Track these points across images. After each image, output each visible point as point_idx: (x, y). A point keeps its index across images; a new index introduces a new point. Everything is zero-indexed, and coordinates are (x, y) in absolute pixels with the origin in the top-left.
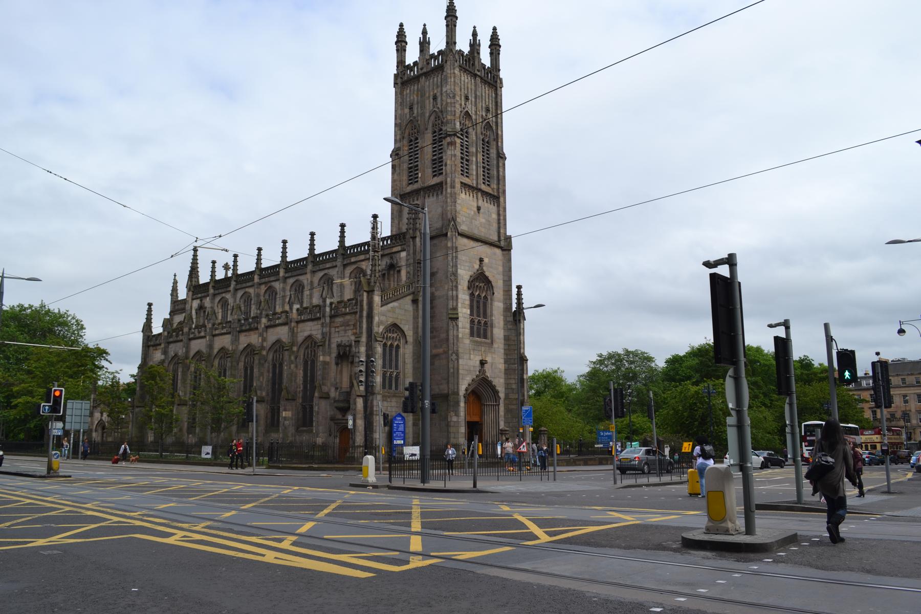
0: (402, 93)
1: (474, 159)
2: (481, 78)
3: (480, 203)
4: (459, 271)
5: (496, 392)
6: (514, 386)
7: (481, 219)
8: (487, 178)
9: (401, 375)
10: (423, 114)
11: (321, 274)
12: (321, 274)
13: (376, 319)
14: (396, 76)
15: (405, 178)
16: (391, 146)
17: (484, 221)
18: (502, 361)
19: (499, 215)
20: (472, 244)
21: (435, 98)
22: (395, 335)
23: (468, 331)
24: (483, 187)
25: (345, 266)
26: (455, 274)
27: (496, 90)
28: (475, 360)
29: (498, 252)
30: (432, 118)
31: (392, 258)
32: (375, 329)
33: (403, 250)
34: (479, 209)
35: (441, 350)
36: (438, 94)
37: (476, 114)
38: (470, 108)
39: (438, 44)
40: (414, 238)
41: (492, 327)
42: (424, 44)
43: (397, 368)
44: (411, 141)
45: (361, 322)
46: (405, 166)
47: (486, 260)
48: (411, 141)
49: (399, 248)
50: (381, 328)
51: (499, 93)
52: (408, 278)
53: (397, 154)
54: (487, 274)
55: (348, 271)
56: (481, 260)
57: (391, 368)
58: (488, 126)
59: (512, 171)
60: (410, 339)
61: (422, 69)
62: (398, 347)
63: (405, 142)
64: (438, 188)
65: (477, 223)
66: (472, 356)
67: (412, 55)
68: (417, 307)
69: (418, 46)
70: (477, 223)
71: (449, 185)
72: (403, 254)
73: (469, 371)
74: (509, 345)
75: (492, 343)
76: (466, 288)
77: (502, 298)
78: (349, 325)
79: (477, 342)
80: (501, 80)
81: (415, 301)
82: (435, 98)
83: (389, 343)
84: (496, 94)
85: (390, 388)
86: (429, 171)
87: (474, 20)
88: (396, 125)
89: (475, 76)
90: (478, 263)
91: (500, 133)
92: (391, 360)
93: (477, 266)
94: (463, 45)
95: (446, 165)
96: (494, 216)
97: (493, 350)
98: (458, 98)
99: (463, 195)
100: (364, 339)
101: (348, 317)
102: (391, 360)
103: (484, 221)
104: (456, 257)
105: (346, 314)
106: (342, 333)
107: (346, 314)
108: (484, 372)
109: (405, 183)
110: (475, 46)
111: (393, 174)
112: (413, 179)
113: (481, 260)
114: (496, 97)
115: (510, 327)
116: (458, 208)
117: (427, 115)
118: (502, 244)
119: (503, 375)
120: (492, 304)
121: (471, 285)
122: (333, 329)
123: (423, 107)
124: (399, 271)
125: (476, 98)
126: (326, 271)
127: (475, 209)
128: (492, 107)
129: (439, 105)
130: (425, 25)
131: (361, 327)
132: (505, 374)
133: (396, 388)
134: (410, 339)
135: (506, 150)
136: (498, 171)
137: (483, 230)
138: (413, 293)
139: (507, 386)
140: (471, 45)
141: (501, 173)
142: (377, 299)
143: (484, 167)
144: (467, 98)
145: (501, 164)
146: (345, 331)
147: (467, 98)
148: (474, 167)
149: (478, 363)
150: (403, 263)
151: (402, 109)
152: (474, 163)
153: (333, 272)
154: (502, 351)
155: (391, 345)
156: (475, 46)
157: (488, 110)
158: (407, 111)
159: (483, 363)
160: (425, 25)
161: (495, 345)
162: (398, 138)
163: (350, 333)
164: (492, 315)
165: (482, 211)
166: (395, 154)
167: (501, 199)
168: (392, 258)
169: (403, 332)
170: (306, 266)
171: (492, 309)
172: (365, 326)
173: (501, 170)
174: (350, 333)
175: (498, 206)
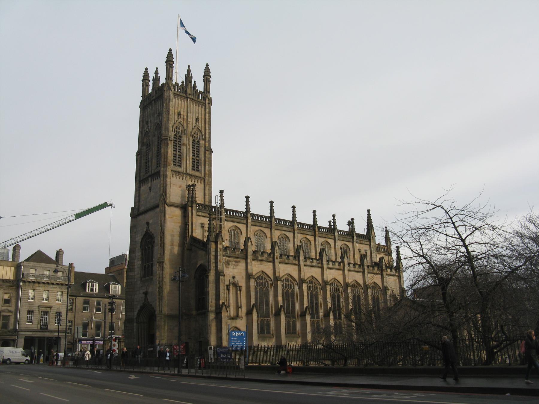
0: (143, 113)
8: (196, 165)
14: (141, 103)
24: (191, 172)
39: (162, 81)
42: (156, 79)
46: (143, 162)
80: (210, 100)
87: (189, 63)
89: (187, 98)
94: (179, 78)
110: (189, 77)
130: (157, 68)
135: (212, 147)
140: (186, 78)
143: (192, 159)
156: (189, 77)
157: (197, 120)
160: (157, 68)
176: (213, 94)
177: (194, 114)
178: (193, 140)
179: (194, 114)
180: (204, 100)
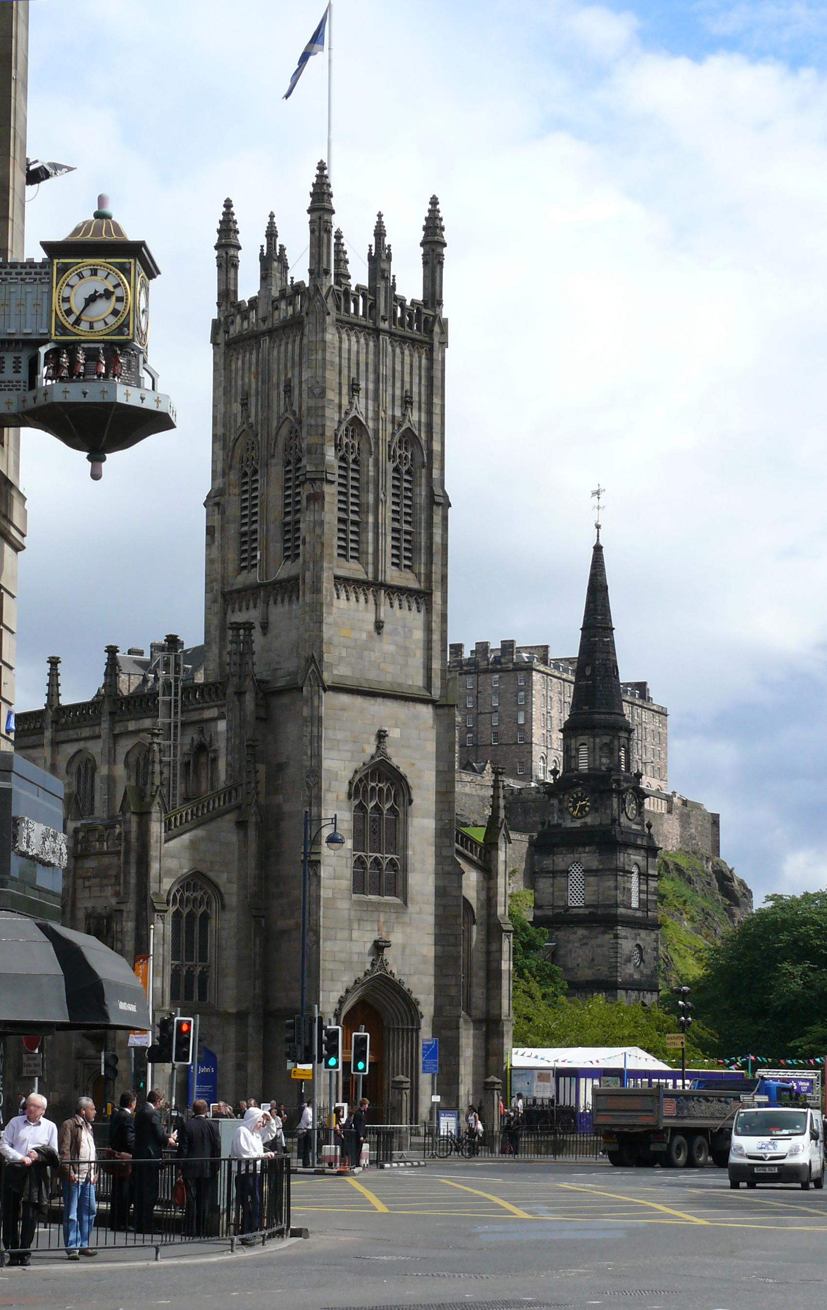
0: (227, 366)
1: (371, 519)
2: (392, 334)
3: (384, 609)
4: (326, 764)
5: (411, 1006)
6: (453, 992)
7: (387, 645)
9: (213, 974)
10: (267, 420)
11: (70, 749)
12: (70, 749)
13: (155, 867)
15: (232, 555)
16: (204, 485)
17: (392, 648)
18: (431, 940)
19: (428, 630)
20: (359, 701)
21: (288, 390)
22: (199, 894)
23: (346, 883)
24: (393, 576)
25: (116, 738)
26: (315, 773)
27: (431, 351)
28: (364, 939)
29: (426, 712)
30: (284, 431)
31: (202, 732)
32: (153, 887)
33: (221, 717)
34: (379, 626)
35: (292, 922)
36: (296, 381)
37: (376, 419)
38: (363, 407)
40: (240, 694)
41: (405, 870)
43: (203, 957)
44: (245, 475)
45: (127, 874)
46: (233, 530)
47: (394, 733)
48: (245, 475)
49: (213, 713)
50: (167, 884)
51: (437, 356)
52: (229, 777)
53: (217, 504)
54: (395, 761)
55: (125, 745)
56: (381, 736)
57: (190, 958)
58: (409, 439)
59: (464, 528)
60: (232, 899)
61: (264, 320)
62: (205, 917)
63: (233, 477)
64: (289, 588)
65: (374, 656)
66: (355, 934)
67: (248, 287)
68: (246, 835)
69: (258, 264)
70: (374, 656)
71: (308, 586)
72: (222, 726)
73: (348, 964)
74: (445, 907)
75: (405, 903)
76: (343, 796)
77: (433, 808)
78: (106, 877)
79: (369, 903)
80: (444, 325)
81: (241, 825)
82: (288, 390)
83: (185, 912)
84: (431, 360)
85: (189, 996)
86: (276, 548)
88: (214, 436)
90: (373, 739)
91: (436, 447)
92: (190, 943)
93: (371, 749)
95: (304, 543)
96: (419, 635)
97: (406, 919)
98: (332, 395)
99: (342, 603)
100: (131, 906)
101: (106, 860)
102: (190, 943)
103: (392, 648)
104: (319, 738)
105: (102, 854)
106: (96, 891)
107: (102, 854)
108: (384, 964)
109: (231, 567)
111: (209, 545)
112: (246, 563)
113: (381, 736)
114: (430, 368)
115: (448, 868)
116: (327, 632)
117: (275, 423)
118: (436, 693)
119: (431, 969)
120: (406, 823)
121: (357, 790)
122: (79, 882)
123: (267, 406)
124: (215, 760)
125: (377, 382)
126: (81, 745)
127: (371, 627)
128: (418, 391)
129: (296, 408)
131: (127, 883)
132: (437, 965)
133: (203, 995)
134: (232, 899)
136: (430, 536)
137: (390, 668)
138: (239, 807)
139: (440, 990)
141: (437, 539)
142: (156, 828)
144: (354, 389)
145: (437, 519)
146: (102, 887)
147: (354, 389)
148: (371, 535)
149: (369, 946)
150: (221, 744)
151: (228, 404)
152: (371, 527)
153: (96, 748)
154: (431, 920)
155: (191, 915)
157: (407, 402)
158: (237, 408)
159: (379, 947)
161: (412, 908)
162: (220, 467)
163: (109, 891)
164: (405, 847)
165: (387, 628)
166: (215, 502)
167: (437, 597)
168: (202, 732)
169: (216, 887)
170: (40, 731)
171: (406, 834)
172: (133, 881)
173: (437, 532)
174: (109, 891)
175: (429, 611)
176: (451, 309)
177: (398, 384)
178: (396, 470)
179: (398, 384)
180: (423, 328)
